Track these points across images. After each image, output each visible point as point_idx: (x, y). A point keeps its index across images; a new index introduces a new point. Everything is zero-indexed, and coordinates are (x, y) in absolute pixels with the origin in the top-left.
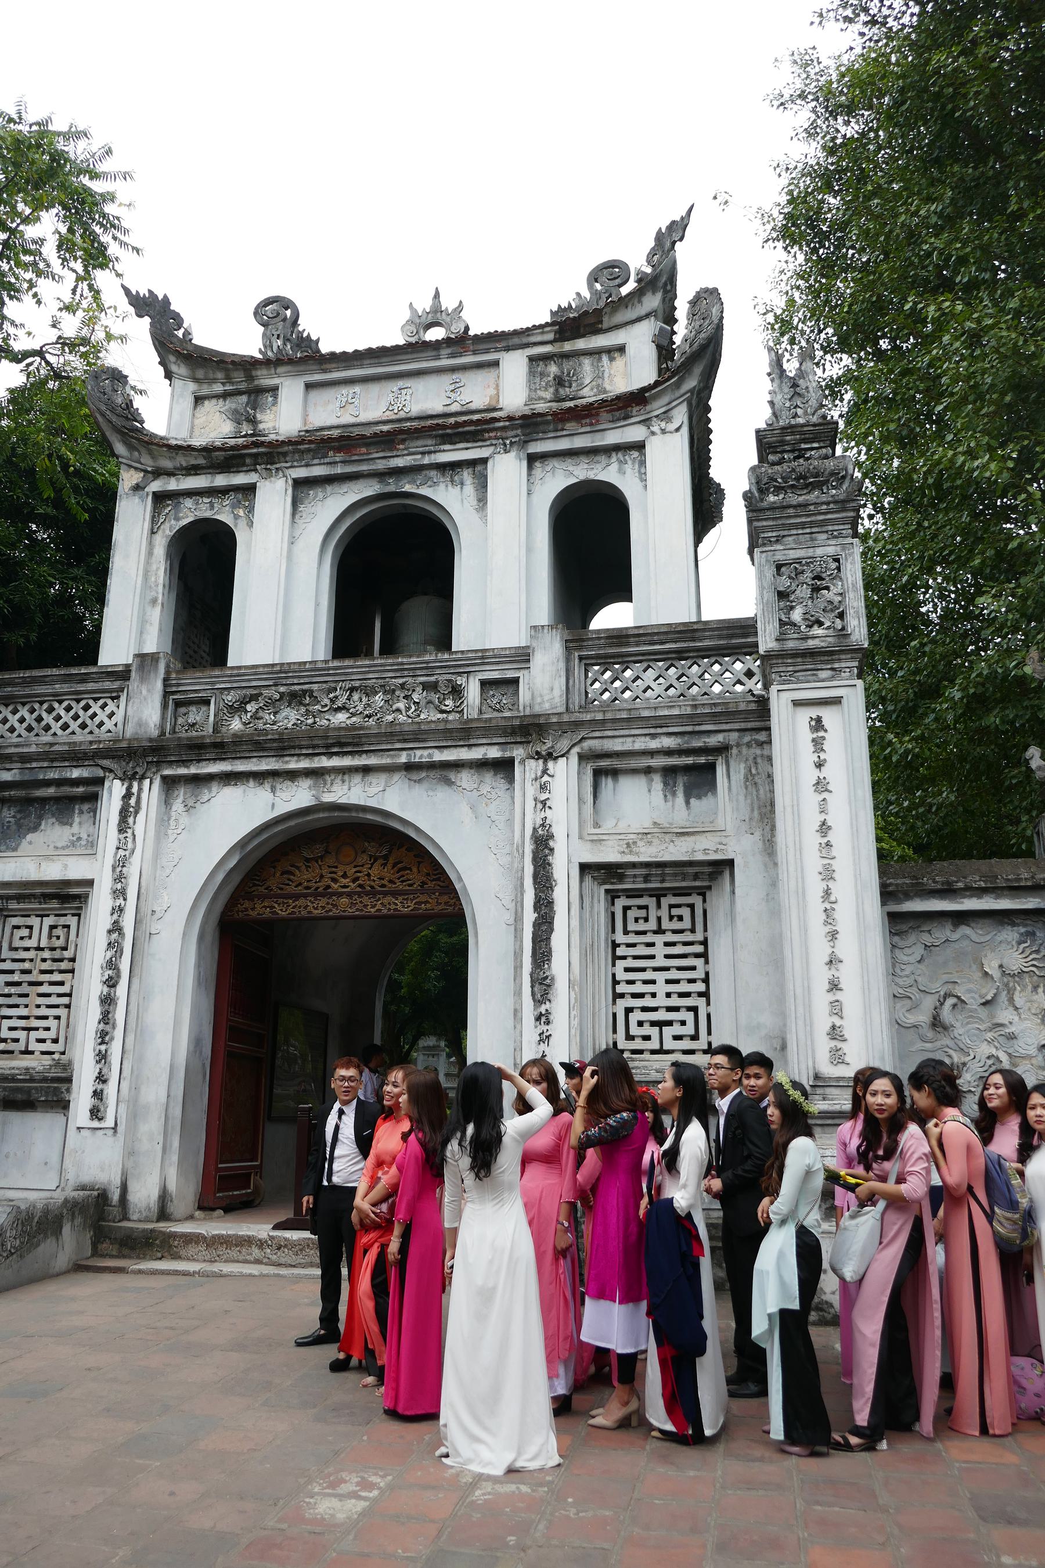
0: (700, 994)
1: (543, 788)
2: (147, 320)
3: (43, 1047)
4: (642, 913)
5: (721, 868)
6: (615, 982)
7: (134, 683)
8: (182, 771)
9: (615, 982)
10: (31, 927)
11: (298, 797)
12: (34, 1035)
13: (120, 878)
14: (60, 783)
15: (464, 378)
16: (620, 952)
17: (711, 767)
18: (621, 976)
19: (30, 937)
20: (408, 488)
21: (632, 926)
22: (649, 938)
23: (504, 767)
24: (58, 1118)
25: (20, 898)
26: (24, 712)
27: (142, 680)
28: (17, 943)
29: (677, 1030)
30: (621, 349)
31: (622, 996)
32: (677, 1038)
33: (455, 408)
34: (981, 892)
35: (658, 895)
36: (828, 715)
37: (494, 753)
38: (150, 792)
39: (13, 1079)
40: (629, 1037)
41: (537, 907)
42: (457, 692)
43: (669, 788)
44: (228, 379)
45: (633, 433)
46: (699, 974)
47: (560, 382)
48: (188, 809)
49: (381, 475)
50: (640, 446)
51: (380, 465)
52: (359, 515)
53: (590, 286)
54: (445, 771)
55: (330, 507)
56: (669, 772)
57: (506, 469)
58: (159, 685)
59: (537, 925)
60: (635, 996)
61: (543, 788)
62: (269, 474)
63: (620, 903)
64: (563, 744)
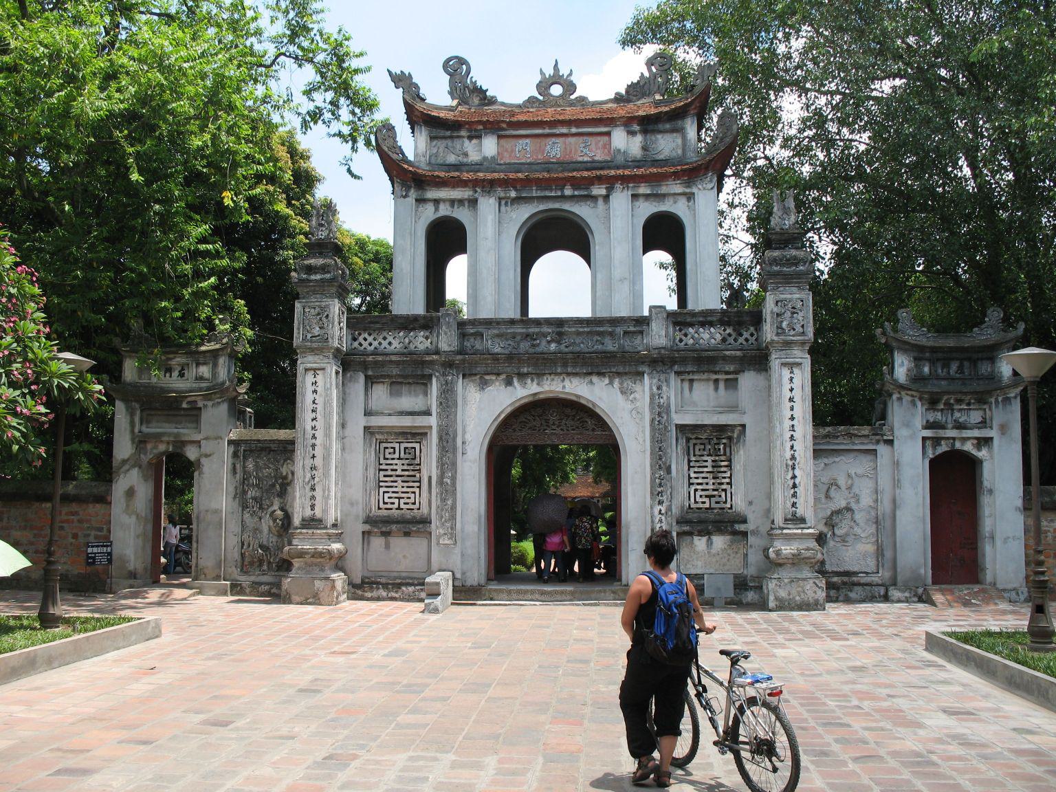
0: (728, 484)
2: (401, 90)
3: (408, 506)
4: (702, 447)
6: (690, 478)
9: (690, 478)
10: (394, 448)
12: (402, 501)
15: (592, 141)
16: (692, 464)
18: (693, 475)
19: (394, 453)
21: (697, 453)
22: (705, 458)
24: (425, 542)
28: (388, 456)
29: (717, 499)
31: (693, 484)
32: (717, 503)
36: (796, 370)
40: (696, 502)
46: (728, 475)
52: (534, 220)
53: (650, 70)
55: (522, 214)
60: (698, 484)
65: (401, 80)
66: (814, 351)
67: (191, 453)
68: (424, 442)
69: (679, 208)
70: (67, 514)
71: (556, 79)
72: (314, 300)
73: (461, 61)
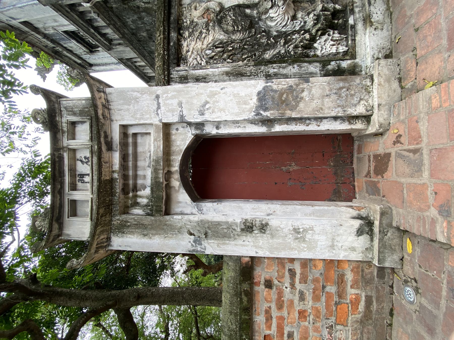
67: (183, 139)
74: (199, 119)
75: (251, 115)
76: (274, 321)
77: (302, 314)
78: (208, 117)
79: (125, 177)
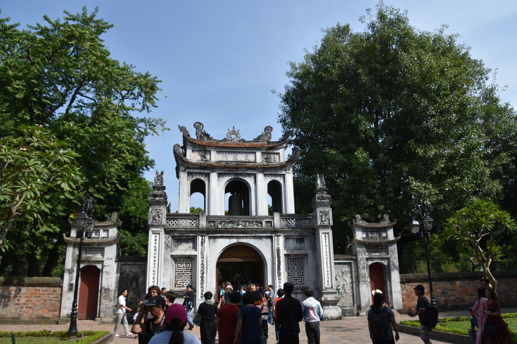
1: (278, 241)
5: (306, 255)
7: (200, 218)
8: (213, 235)
11: (234, 241)
13: (202, 255)
14: (186, 236)
17: (304, 239)
20: (241, 177)
23: (271, 238)
25: (180, 258)
26: (176, 221)
27: (202, 217)
30: (279, 153)
33: (247, 160)
34: (342, 260)
35: (295, 259)
37: (269, 235)
38: (207, 239)
39: (183, 291)
41: (278, 261)
42: (261, 223)
43: (297, 242)
44: (200, 148)
45: (284, 172)
47: (266, 158)
48: (213, 242)
49: (235, 174)
50: (284, 175)
51: (236, 172)
54: (260, 238)
55: (226, 179)
56: (297, 239)
57: (260, 176)
58: (205, 218)
59: (278, 264)
61: (278, 241)
62: (213, 172)
63: (289, 260)
64: (281, 234)
65: (182, 129)
66: (333, 228)
67: (99, 266)
68: (193, 262)
69: (280, 180)
70: (42, 291)
71: (234, 132)
72: (157, 207)
73: (201, 124)
74: (104, 271)
75: (103, 286)
76: (43, 292)
77: (45, 300)
78: (104, 274)
79: (90, 248)
